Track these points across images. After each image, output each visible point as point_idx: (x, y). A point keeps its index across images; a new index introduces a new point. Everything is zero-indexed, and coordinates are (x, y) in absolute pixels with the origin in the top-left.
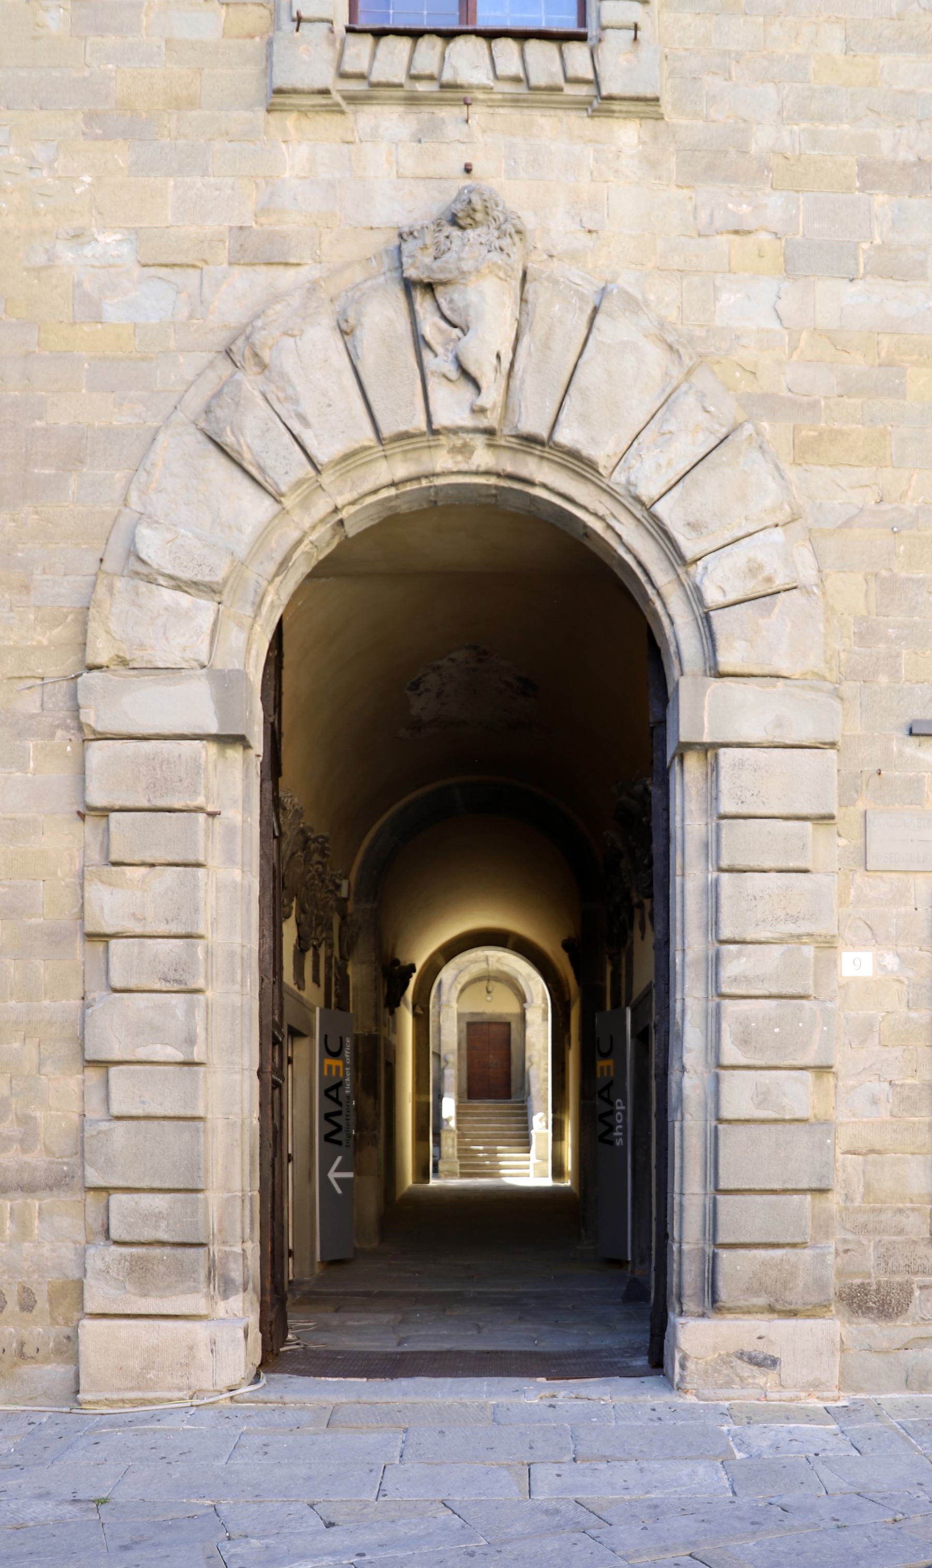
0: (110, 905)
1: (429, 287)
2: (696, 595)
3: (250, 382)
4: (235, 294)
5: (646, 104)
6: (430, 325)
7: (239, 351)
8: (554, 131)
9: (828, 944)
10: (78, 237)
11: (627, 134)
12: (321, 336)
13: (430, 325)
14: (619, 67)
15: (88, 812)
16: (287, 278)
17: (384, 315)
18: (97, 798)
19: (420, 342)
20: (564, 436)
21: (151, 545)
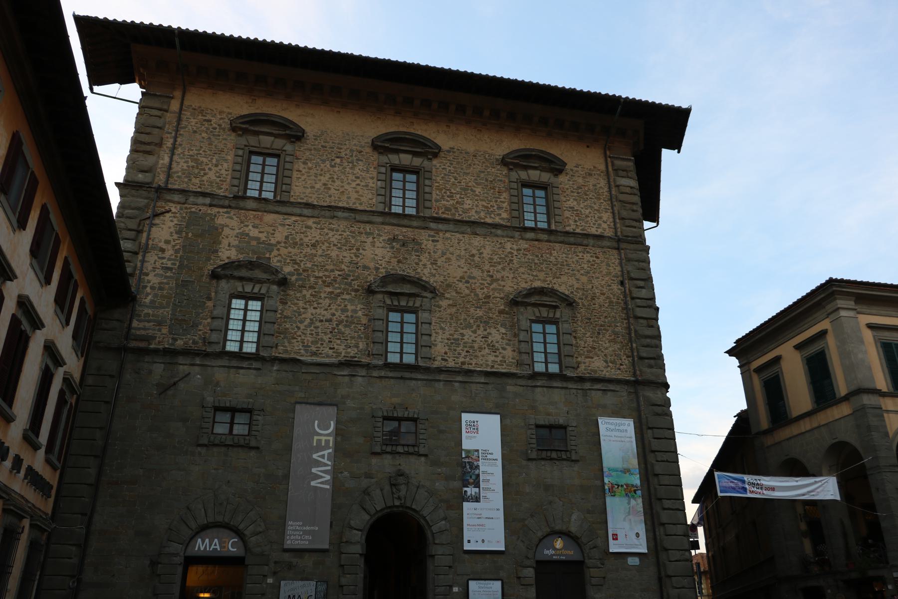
0: (344, 581)
1: (394, 485)
2: (432, 531)
3: (367, 498)
4: (365, 483)
5: (426, 456)
6: (394, 490)
7: (366, 492)
8: (413, 459)
9: (451, 587)
10: (342, 473)
11: (423, 459)
12: (378, 491)
13: (394, 490)
14: (422, 450)
15: (342, 566)
16: (373, 480)
17: (387, 488)
18: (342, 563)
19: (393, 493)
20: (413, 507)
21: (352, 523)
